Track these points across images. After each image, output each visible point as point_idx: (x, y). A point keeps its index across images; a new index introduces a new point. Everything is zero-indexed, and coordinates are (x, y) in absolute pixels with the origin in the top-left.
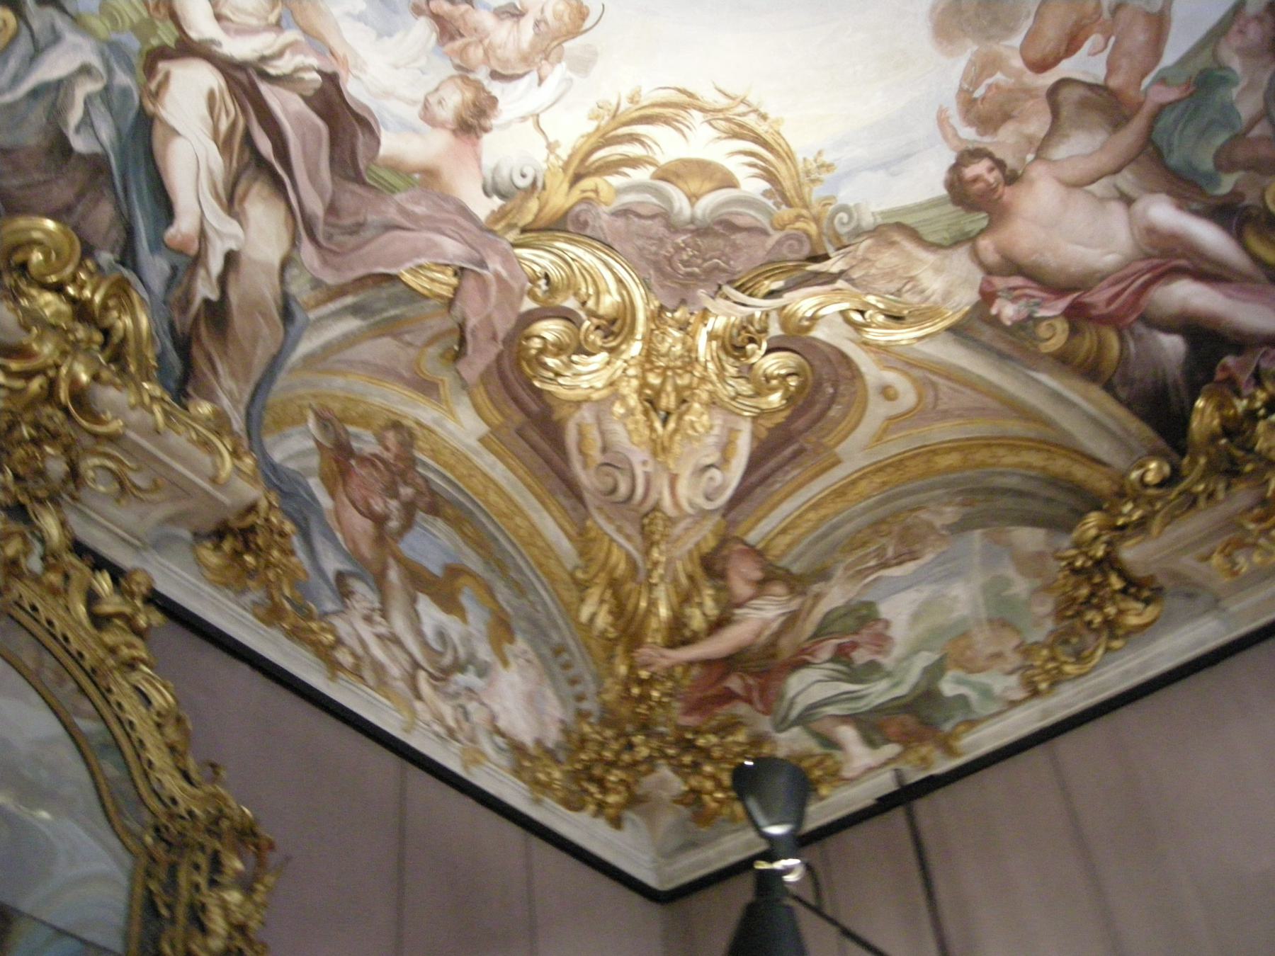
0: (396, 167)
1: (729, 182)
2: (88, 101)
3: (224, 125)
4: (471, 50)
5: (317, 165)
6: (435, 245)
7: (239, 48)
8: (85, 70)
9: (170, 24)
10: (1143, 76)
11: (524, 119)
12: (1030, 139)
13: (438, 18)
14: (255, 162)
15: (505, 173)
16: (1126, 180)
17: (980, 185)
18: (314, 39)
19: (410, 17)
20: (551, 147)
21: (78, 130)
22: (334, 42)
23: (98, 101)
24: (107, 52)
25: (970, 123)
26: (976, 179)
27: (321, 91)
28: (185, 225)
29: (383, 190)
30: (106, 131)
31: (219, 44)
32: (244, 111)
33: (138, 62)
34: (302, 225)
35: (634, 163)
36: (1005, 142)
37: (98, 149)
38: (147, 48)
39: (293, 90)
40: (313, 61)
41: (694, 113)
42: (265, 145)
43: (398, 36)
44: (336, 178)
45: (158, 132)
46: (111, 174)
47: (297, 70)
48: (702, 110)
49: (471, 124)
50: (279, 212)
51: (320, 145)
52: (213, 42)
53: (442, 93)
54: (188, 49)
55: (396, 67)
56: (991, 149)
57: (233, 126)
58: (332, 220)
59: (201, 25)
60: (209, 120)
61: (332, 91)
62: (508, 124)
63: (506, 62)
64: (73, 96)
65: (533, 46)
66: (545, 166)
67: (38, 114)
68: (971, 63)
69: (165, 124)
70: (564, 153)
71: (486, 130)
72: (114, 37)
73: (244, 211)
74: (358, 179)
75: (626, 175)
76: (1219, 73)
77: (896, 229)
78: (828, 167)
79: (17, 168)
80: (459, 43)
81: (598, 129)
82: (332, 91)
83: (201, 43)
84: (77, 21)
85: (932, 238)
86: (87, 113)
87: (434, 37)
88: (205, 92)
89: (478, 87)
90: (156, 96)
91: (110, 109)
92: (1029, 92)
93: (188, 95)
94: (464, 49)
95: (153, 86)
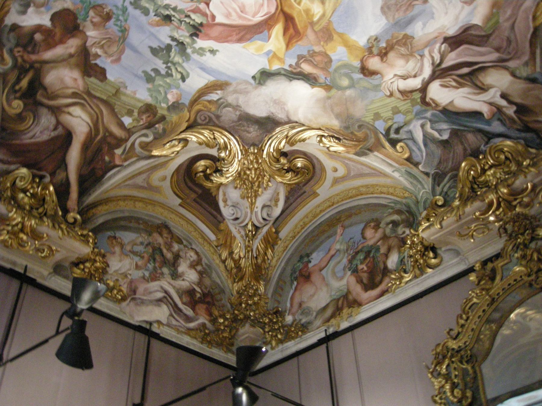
2: (432, 128)
3: (454, 84)
5: (479, 52)
7: (427, 72)
8: (422, 126)
9: (414, 94)
14: (470, 76)
18: (430, 44)
21: (441, 135)
22: (432, 36)
23: (434, 125)
24: (418, 117)
27: (450, 45)
28: (485, 109)
30: (444, 126)
31: (424, 78)
33: (424, 108)
34: (500, 64)
37: (449, 131)
38: (420, 103)
39: (447, 55)
40: (437, 46)
42: (465, 70)
43: (434, 11)
45: (450, 108)
46: (459, 130)
47: (440, 52)
50: (492, 71)
51: (471, 49)
52: (423, 80)
54: (424, 89)
57: (455, 80)
59: (416, 83)
60: (451, 89)
61: (450, 41)
64: (430, 133)
67: (432, 147)
69: (447, 105)
72: (414, 113)
73: (487, 85)
74: (488, 36)
79: (447, 161)
82: (450, 41)
83: (422, 84)
84: (406, 124)
86: (436, 130)
88: (440, 87)
90: (437, 105)
91: (437, 122)
93: (441, 94)
95: (434, 105)
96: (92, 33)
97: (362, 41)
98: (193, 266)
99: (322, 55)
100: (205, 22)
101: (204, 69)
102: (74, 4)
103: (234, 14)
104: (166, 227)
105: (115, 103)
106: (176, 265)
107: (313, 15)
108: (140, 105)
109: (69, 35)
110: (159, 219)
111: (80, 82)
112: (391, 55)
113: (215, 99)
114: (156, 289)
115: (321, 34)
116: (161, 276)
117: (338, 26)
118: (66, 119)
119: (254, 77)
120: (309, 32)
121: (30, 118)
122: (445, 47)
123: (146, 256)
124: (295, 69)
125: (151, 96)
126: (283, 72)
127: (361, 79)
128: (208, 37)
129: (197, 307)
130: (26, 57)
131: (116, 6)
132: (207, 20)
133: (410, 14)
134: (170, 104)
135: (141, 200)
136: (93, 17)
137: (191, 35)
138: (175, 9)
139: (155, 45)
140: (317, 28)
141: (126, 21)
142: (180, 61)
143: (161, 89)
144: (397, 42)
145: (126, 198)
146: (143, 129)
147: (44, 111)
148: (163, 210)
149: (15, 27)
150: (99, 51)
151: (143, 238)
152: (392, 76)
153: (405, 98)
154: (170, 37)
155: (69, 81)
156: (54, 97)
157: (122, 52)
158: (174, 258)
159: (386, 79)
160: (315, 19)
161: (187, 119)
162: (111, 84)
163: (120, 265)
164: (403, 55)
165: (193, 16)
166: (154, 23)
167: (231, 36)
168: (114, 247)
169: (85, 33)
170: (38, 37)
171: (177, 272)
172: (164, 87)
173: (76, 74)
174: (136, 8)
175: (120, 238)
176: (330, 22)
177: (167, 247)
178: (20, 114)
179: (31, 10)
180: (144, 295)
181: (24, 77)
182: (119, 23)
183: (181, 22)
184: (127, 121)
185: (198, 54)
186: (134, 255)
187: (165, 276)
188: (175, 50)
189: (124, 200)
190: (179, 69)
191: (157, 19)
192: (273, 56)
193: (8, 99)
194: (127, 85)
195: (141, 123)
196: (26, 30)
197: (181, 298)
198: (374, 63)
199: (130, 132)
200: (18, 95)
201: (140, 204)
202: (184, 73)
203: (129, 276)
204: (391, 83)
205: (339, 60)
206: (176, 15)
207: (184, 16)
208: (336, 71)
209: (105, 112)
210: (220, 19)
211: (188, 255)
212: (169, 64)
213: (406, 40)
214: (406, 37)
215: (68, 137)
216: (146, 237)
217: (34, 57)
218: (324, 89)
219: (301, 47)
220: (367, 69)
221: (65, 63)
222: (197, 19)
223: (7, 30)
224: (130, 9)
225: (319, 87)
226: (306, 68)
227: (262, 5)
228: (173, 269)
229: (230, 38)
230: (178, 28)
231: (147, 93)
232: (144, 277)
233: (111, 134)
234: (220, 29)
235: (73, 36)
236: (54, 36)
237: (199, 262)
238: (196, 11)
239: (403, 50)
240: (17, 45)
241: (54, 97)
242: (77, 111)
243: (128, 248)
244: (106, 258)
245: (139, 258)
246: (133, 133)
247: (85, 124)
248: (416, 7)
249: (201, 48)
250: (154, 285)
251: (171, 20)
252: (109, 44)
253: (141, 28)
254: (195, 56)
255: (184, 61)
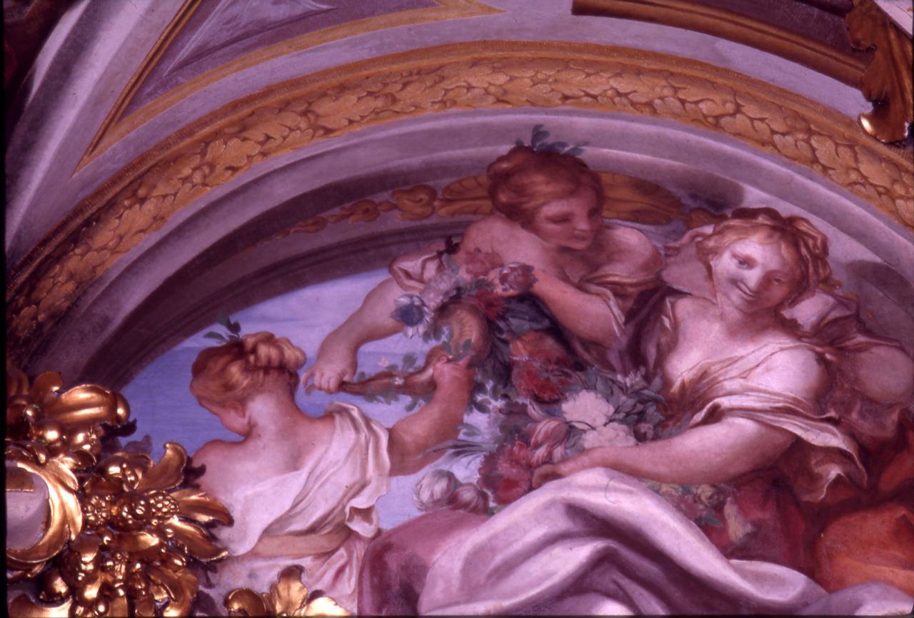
98: (764, 314)
104: (547, 156)
106: (652, 352)
110: (497, 133)
114: (537, 533)
116: (558, 452)
123: (445, 372)
129: (833, 536)
135: (342, 82)
145: (242, 116)
148: (501, 79)
151: (426, 277)
158: (630, 315)
163: (296, 482)
168: (240, 403)
171: (667, 383)
175: (269, 339)
177: (576, 273)
180: (471, 596)
186: (370, 397)
187: (589, 440)
189: (242, 128)
197: (710, 528)
201: (350, 104)
203: (358, 526)
211: (725, 264)
216: (431, 268)
228: (632, 380)
232: (452, 499)
237: (807, 266)
243: (329, 374)
244: (204, 480)
245: (407, 400)
250: (527, 517)
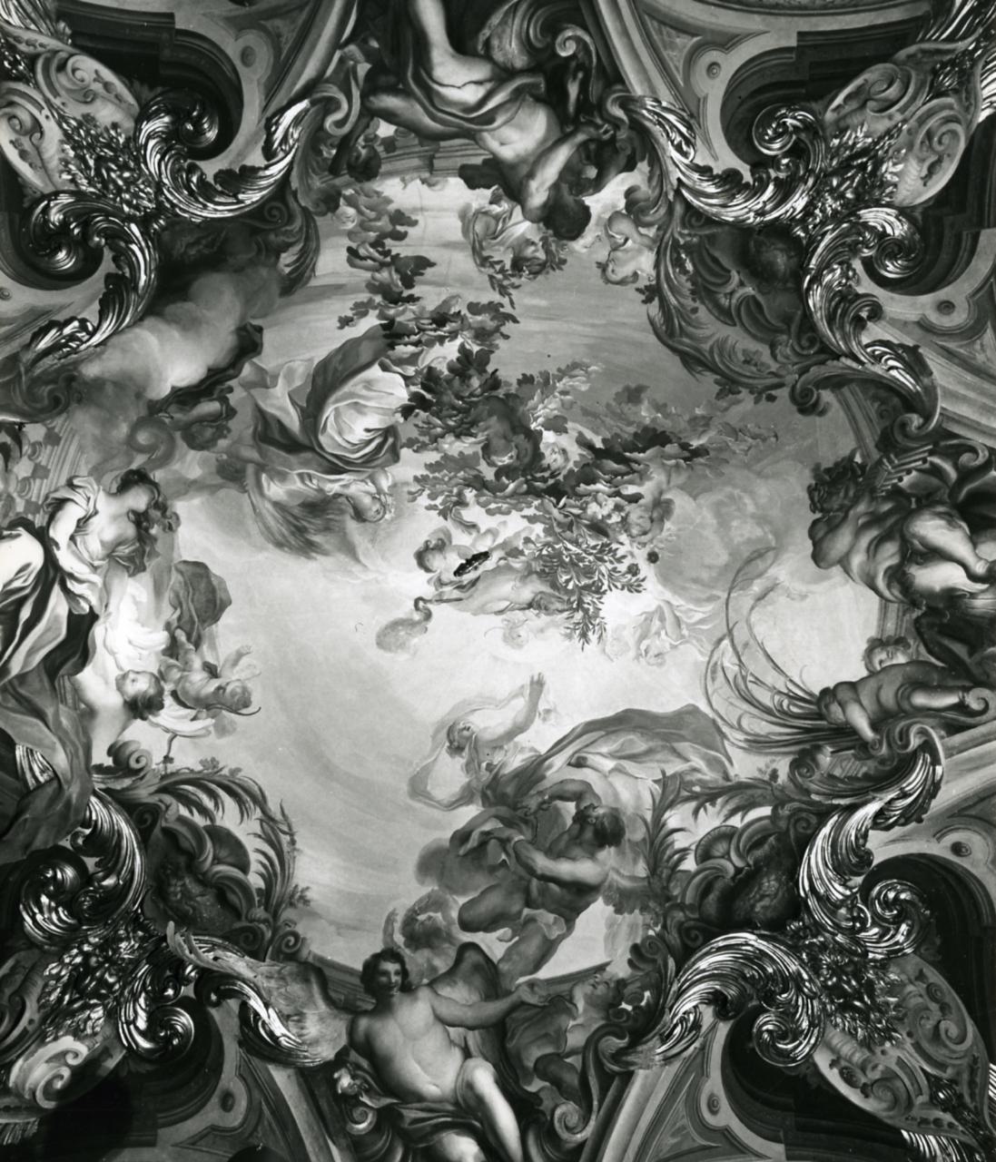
0: (77, 691)
1: (244, 868)
3: (17, 584)
4: (175, 670)
6: (53, 749)
7: (66, 559)
9: (47, 517)
10: (523, 974)
11: (167, 730)
12: (433, 969)
13: (173, 639)
15: (132, 748)
16: (473, 1039)
17: (384, 979)
18: (106, 589)
19: (161, 625)
20: (167, 759)
25: (404, 935)
26: (386, 973)
27: (81, 617)
29: (57, 694)
31: (58, 548)
32: (34, 589)
33: (12, 516)
35: (204, 811)
36: (417, 960)
40: (94, 602)
41: (258, 810)
42: (25, 613)
43: (146, 629)
44: (42, 667)
47: (80, 596)
48: (264, 812)
49: (140, 707)
51: (50, 642)
52: (57, 545)
53: (139, 677)
55: (130, 642)
56: (406, 959)
57: (22, 589)
58: (16, 683)
59: (62, 530)
60: (12, 576)
62: (157, 725)
63: (186, 693)
65: (207, 697)
66: (154, 766)
68: (429, 896)
70: (171, 768)
71: (144, 719)
75: (191, 812)
76: (569, 1005)
77: (318, 973)
78: (306, 902)
80: (172, 661)
81: (200, 772)
85: (333, 995)
87: (164, 646)
89: (160, 692)
92: (450, 938)
94: (170, 667)
96: (521, 228)
97: (181, 507)
99: (208, 442)
100: (390, 352)
101: (337, 289)
102: (572, 252)
103: (364, 392)
105: (421, 144)
107: (272, 479)
108: (384, 168)
109: (551, 202)
111: (493, 144)
112: (131, 531)
113: (283, 255)
115: (238, 466)
117: (231, 493)
118: (481, 71)
119: (260, 330)
120: (252, 454)
121: (535, 36)
122: (83, 609)
124: (222, 390)
125: (378, 193)
126: (231, 372)
127: (130, 463)
128: (368, 336)
130: (592, 130)
131: (517, 287)
132: (388, 357)
133: (168, 595)
134: (342, 201)
136: (536, 251)
137: (392, 321)
138: (441, 340)
139: (429, 272)
140: (250, 469)
141: (491, 277)
142: (377, 275)
143: (372, 215)
144: (144, 552)
146: (351, 132)
147: (520, 61)
149: (630, 167)
150: (496, 209)
152: (98, 507)
153: (49, 501)
154: (418, 299)
155: (509, 133)
156: (517, 95)
157: (465, 231)
159: (102, 493)
160: (264, 477)
161: (299, 196)
162: (447, 172)
164: (120, 544)
165: (411, 349)
166: (453, 302)
167: (342, 361)
169: (533, 221)
170: (592, 172)
172: (371, 220)
173: (507, 153)
174: (491, 303)
176: (244, 490)
178: (555, 37)
179: (622, 204)
181: (578, 99)
182: (498, 267)
183: (421, 330)
184: (385, 130)
185: (362, 303)
188: (397, 286)
190: (370, 262)
191: (453, 311)
192: (264, 380)
193: (585, 45)
194: (425, 186)
195: (362, 138)
196: (613, 171)
198: (138, 499)
199: (369, 114)
200: (573, 64)
202: (358, 262)
204: (89, 499)
205: (183, 457)
206: (432, 333)
207: (424, 339)
208: (172, 440)
209: (427, 121)
210: (375, 372)
212: (388, 259)
213: (134, 565)
214: (142, 569)
215: (462, 43)
217: (581, 137)
218: (157, 402)
219: (242, 425)
220: (136, 483)
221: (531, 159)
222: (404, 350)
223: (638, 157)
224: (495, 297)
225: (168, 397)
226: (209, 407)
227: (340, 433)
229: (340, 357)
230: (417, 319)
231: (385, 194)
233: (393, 90)
234: (364, 359)
235: (545, 205)
236: (571, 189)
238: (413, 359)
239: (125, 550)
240: (613, 138)
241: (517, 95)
242: (471, 95)
246: (361, 115)
247: (446, 82)
248: (170, 610)
249: (364, 314)
251: (434, 321)
252: (492, 229)
253: (465, 282)
254: (364, 297)
255: (373, 278)
